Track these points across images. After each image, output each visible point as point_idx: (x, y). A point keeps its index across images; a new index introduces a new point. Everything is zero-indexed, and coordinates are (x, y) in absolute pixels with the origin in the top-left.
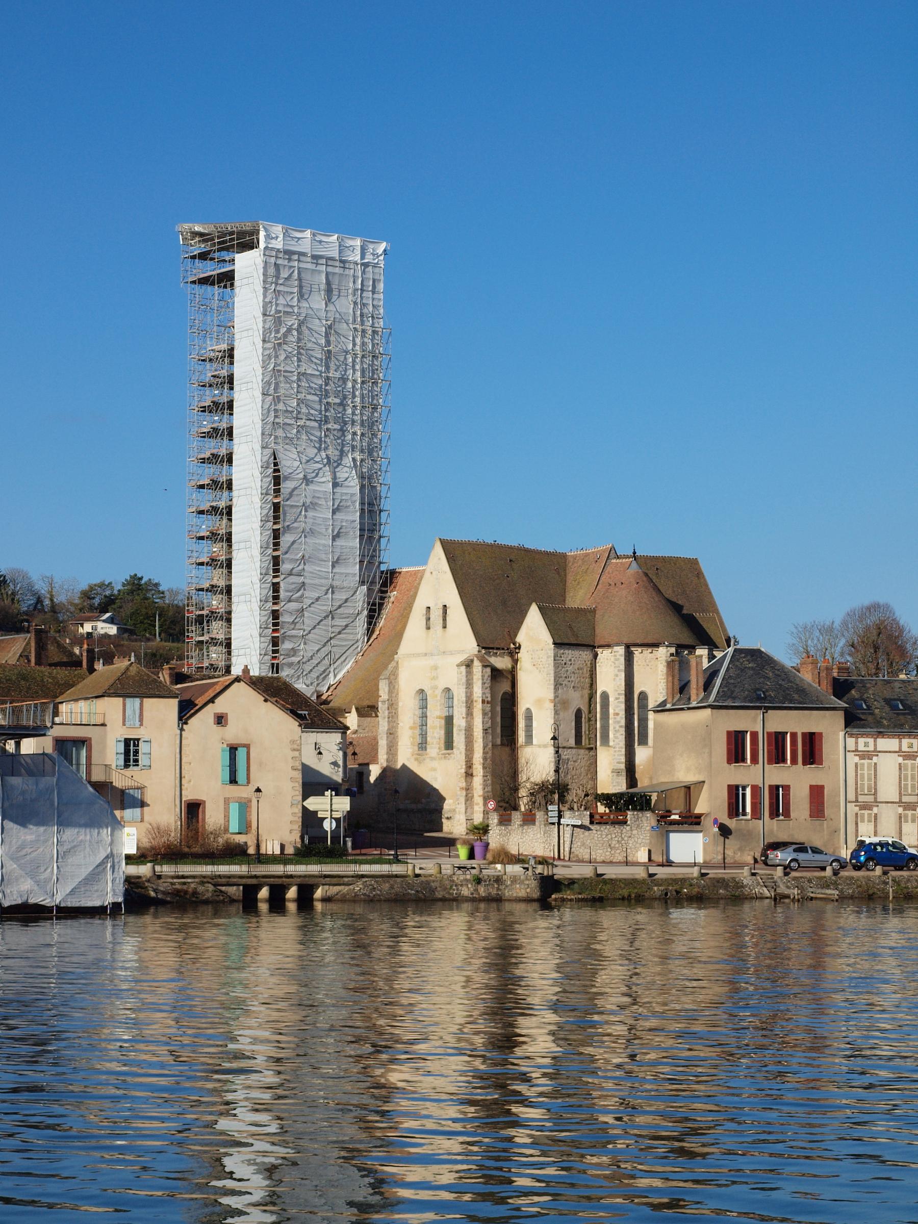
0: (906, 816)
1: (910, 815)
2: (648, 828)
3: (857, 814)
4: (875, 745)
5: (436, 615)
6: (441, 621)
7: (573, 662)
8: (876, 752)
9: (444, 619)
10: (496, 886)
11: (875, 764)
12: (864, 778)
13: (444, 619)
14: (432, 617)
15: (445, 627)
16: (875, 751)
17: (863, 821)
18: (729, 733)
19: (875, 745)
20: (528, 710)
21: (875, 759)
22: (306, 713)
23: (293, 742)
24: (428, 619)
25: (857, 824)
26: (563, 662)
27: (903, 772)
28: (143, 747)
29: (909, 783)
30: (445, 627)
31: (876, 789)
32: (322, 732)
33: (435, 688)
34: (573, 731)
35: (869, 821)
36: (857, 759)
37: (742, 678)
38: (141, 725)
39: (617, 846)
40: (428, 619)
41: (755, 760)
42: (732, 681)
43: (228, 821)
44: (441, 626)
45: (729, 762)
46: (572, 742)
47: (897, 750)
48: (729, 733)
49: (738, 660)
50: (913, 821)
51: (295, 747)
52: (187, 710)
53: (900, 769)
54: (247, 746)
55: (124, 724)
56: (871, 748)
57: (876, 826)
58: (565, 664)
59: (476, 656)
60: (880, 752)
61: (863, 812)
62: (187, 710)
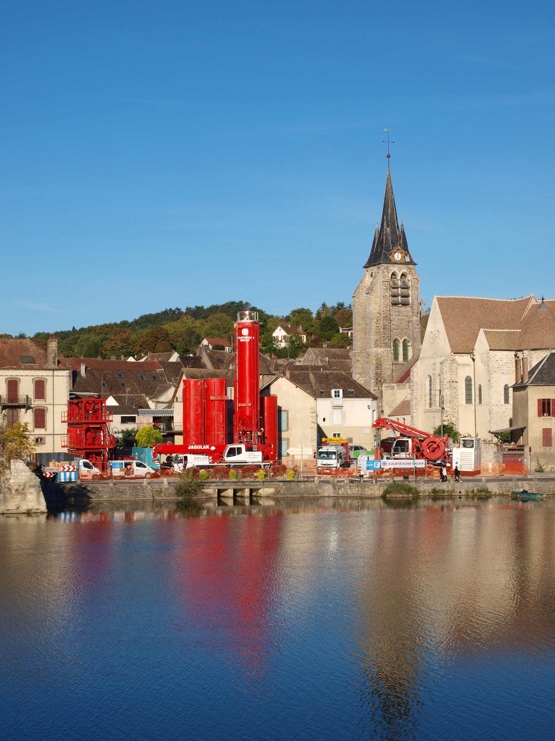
2: (493, 453)
7: (502, 359)
10: (357, 489)
18: (539, 400)
20: (480, 386)
22: (353, 390)
23: (311, 409)
26: (496, 360)
32: (360, 400)
33: (434, 374)
37: (551, 370)
42: (545, 371)
45: (539, 415)
48: (539, 400)
49: (551, 360)
51: (313, 411)
54: (288, 411)
58: (497, 361)
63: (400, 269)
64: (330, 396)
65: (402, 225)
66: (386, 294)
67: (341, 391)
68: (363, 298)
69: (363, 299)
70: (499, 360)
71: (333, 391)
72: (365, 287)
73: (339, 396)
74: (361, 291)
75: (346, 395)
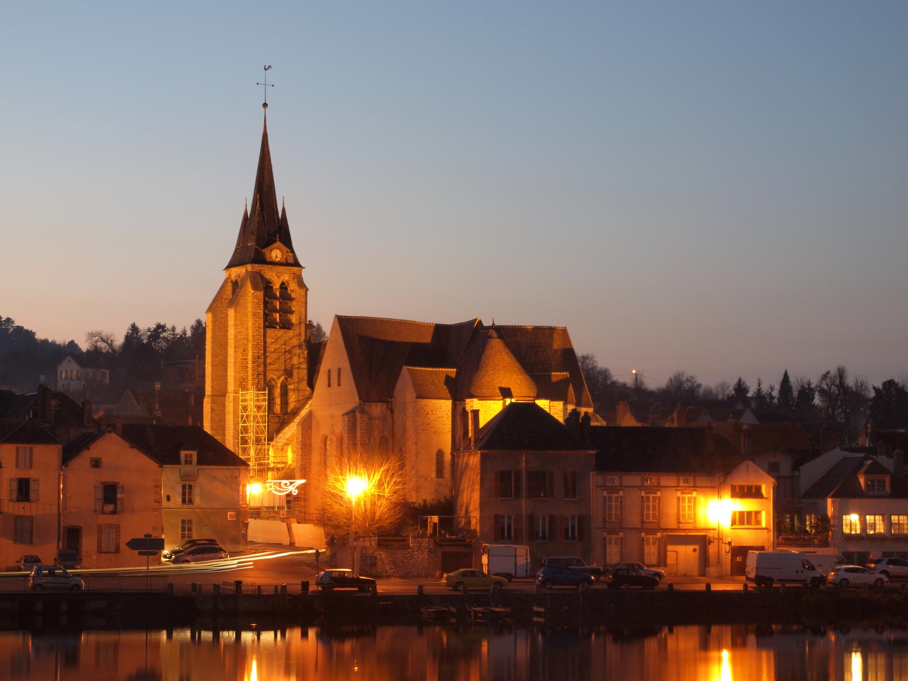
0: (648, 540)
1: (651, 539)
3: (605, 539)
4: (621, 482)
5: (334, 376)
6: (337, 380)
8: (622, 487)
9: (339, 379)
11: (621, 497)
12: (611, 508)
13: (339, 379)
14: (332, 377)
15: (339, 385)
16: (621, 486)
17: (610, 543)
19: (621, 482)
21: (621, 493)
24: (329, 378)
25: (605, 546)
27: (645, 504)
28: (32, 486)
29: (651, 512)
30: (339, 385)
31: (621, 517)
34: (434, 467)
35: (616, 543)
36: (605, 493)
38: (31, 467)
39: (400, 564)
40: (329, 378)
41: (518, 494)
43: (101, 543)
44: (337, 383)
46: (434, 475)
47: (640, 485)
50: (654, 543)
51: (157, 484)
52: (68, 456)
53: (643, 501)
55: (17, 467)
56: (617, 483)
57: (621, 548)
59: (357, 408)
60: (625, 487)
61: (610, 536)
62: (68, 456)
63: (279, 274)
64: (179, 463)
65: (284, 210)
66: (259, 311)
67: (194, 454)
68: (222, 316)
69: (222, 318)
70: (430, 412)
71: (183, 453)
72: (225, 299)
73: (191, 463)
74: (219, 305)
75: (200, 462)
